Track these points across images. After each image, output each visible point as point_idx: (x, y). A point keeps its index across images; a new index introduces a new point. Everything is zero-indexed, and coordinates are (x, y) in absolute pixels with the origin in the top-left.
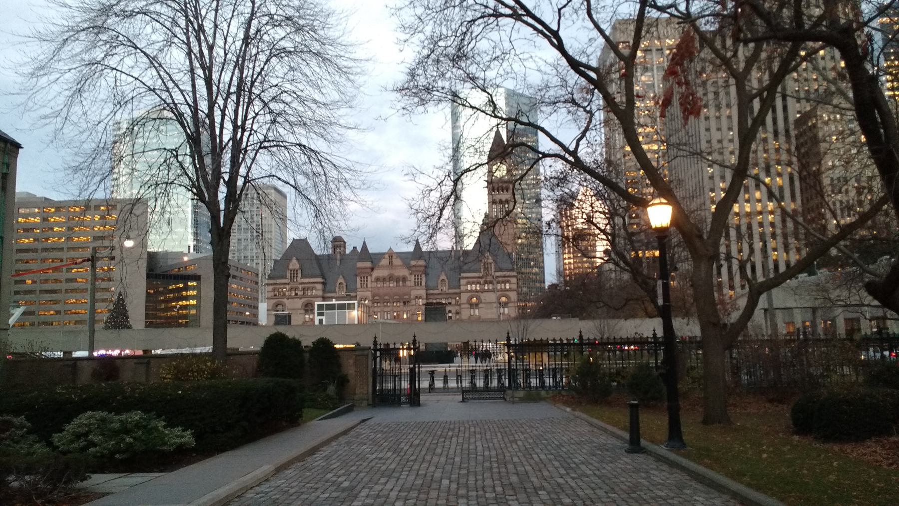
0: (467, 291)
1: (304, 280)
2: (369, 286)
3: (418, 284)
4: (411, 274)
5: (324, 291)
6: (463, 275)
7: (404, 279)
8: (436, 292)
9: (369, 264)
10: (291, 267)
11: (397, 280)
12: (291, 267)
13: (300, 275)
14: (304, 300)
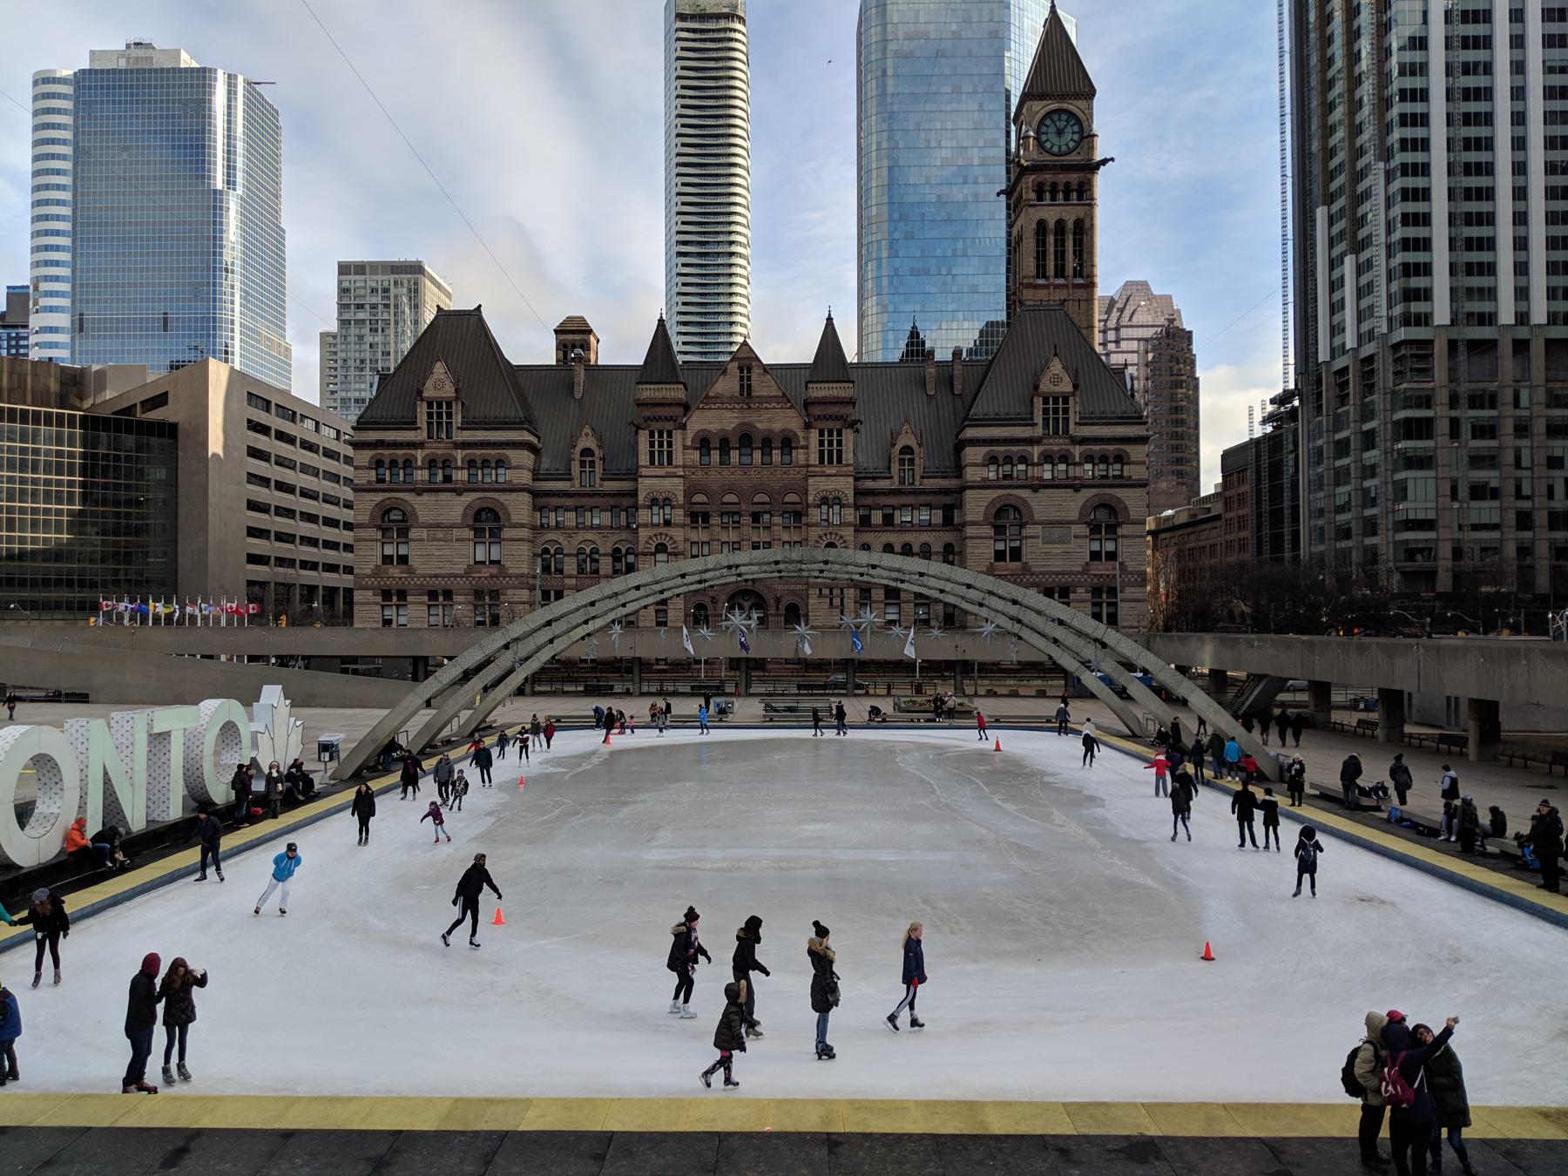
0: (985, 485)
1: (468, 436)
2: (678, 458)
3: (832, 456)
4: (807, 426)
6: (971, 433)
7: (788, 443)
9: (676, 392)
11: (767, 444)
13: (457, 419)
14: (469, 497)
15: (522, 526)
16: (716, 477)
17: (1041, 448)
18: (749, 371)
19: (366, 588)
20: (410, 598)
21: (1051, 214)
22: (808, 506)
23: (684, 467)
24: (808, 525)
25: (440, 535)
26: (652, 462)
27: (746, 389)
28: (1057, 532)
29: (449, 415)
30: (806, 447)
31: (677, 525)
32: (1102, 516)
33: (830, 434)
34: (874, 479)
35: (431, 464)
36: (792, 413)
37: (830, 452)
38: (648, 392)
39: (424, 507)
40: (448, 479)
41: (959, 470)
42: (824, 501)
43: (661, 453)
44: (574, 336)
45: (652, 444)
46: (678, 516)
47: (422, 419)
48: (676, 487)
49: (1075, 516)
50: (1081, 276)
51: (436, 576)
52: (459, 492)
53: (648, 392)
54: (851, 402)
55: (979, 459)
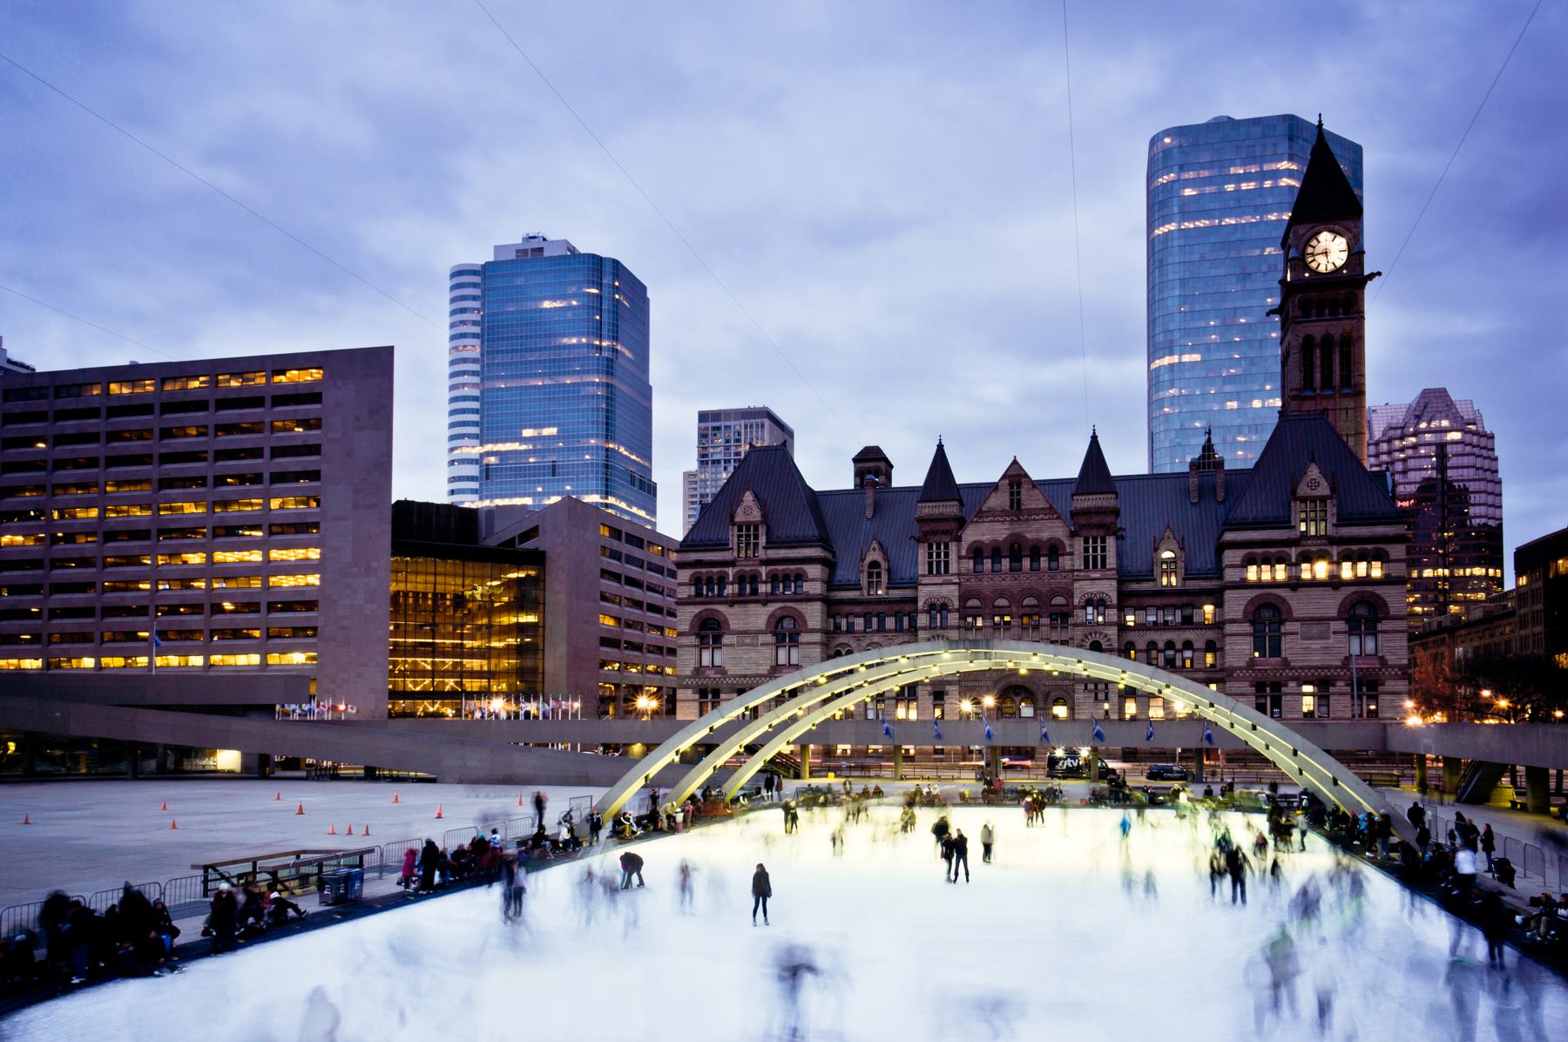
0: (1244, 584)
2: (953, 568)
3: (1094, 562)
4: (1073, 535)
5: (830, 584)
6: (1229, 536)
7: (1055, 550)
8: (1146, 586)
9: (950, 508)
10: (739, 518)
11: (1035, 551)
12: (739, 518)
13: (762, 540)
14: (772, 607)
15: (816, 631)
16: (987, 584)
17: (1300, 549)
18: (1019, 486)
19: (687, 687)
20: (723, 696)
21: (1317, 329)
22: (1075, 607)
23: (959, 575)
24: (1076, 625)
25: (748, 641)
26: (930, 571)
27: (1016, 505)
28: (1315, 629)
29: (756, 537)
30: (1072, 554)
31: (952, 628)
32: (1362, 611)
33: (1095, 541)
34: (1138, 581)
35: (741, 579)
36: (1059, 523)
37: (1095, 558)
38: (927, 509)
39: (736, 617)
40: (755, 591)
41: (1219, 572)
42: (1089, 602)
43: (938, 563)
44: (872, 463)
45: (930, 556)
46: (953, 618)
47: (733, 542)
48: (951, 593)
49: (1334, 612)
50: (1349, 386)
51: (745, 676)
52: (765, 603)
53: (927, 509)
54: (1116, 512)
55: (1238, 561)
